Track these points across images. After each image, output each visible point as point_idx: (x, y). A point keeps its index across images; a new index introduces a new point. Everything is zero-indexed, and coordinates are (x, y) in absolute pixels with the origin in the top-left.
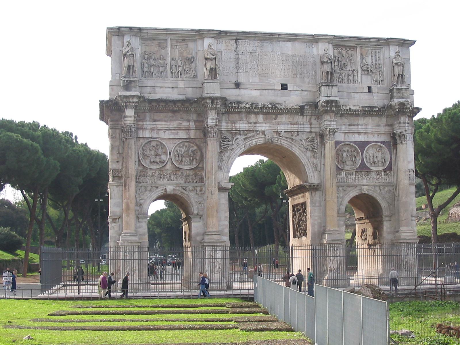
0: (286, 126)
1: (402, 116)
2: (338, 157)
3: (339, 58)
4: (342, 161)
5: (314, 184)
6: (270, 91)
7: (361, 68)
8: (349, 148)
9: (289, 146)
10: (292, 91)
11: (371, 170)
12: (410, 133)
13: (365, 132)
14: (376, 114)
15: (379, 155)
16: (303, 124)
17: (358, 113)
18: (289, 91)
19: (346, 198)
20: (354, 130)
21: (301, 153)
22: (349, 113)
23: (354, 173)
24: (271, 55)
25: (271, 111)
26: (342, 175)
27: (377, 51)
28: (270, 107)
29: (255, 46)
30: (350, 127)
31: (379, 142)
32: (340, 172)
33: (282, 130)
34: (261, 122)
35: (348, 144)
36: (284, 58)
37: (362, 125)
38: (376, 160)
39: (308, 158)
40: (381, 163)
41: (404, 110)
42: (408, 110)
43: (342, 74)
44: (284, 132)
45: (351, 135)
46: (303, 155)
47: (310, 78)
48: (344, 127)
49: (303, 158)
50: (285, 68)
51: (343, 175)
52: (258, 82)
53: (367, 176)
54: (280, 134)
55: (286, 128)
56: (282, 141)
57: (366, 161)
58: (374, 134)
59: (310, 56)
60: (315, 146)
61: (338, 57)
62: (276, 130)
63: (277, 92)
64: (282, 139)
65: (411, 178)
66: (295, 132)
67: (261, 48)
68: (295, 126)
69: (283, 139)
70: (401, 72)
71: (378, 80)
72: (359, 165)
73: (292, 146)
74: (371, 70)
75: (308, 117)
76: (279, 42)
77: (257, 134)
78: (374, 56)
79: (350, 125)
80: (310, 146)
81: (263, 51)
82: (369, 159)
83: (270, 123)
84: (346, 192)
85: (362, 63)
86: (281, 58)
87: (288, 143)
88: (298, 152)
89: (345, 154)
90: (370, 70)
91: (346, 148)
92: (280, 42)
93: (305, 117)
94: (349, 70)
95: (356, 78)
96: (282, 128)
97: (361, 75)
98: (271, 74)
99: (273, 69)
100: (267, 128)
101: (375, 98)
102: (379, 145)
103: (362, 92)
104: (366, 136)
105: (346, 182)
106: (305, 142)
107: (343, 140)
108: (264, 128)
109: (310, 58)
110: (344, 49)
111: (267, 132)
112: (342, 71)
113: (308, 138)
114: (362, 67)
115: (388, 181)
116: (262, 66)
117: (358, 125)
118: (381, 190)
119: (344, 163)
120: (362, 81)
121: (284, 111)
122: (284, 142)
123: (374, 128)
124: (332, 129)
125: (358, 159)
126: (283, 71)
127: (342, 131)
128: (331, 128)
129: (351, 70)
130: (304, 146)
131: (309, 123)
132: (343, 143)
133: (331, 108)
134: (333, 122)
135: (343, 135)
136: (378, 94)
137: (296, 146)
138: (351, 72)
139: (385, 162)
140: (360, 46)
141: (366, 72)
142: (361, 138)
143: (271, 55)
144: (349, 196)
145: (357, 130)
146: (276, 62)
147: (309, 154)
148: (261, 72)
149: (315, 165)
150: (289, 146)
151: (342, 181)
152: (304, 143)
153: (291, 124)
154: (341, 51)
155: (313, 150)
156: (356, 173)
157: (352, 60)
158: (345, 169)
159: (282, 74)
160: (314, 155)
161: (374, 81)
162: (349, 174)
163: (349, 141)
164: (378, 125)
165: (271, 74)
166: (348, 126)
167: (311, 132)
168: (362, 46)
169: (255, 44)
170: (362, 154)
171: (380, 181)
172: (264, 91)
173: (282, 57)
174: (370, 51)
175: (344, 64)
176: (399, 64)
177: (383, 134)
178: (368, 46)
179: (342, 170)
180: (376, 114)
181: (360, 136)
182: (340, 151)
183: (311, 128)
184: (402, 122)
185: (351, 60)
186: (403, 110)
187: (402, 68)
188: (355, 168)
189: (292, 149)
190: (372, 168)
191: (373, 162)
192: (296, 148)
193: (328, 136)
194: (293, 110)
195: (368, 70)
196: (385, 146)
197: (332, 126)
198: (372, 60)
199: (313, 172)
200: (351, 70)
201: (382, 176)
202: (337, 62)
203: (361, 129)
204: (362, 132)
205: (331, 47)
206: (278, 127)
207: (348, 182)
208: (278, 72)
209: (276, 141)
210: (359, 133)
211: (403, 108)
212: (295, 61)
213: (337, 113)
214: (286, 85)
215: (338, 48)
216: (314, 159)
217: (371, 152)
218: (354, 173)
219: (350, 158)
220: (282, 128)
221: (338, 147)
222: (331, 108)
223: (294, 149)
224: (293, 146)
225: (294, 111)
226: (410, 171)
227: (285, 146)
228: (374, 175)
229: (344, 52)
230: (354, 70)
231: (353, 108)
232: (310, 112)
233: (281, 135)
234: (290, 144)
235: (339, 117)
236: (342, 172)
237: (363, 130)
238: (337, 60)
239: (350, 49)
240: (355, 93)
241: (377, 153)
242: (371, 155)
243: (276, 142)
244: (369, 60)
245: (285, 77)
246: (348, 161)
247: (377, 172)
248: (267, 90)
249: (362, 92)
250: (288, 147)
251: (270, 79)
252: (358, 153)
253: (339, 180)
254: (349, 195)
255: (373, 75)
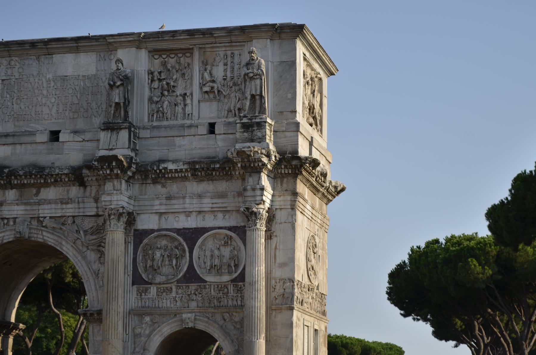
0: (53, 206)
1: (250, 176)
2: (146, 261)
3: (162, 74)
4: (152, 266)
5: (91, 312)
6: (29, 146)
7: (201, 88)
8: (168, 241)
9: (57, 243)
10: (68, 143)
11: (206, 282)
12: (289, 207)
13: (198, 210)
14: (218, 174)
15: (226, 252)
16: (84, 202)
17: (183, 175)
18: (61, 144)
19: (154, 336)
20: (176, 207)
21: (77, 255)
22: (166, 176)
23: (174, 289)
24: (36, 81)
25: (25, 182)
26: (150, 293)
27: (236, 53)
28: (22, 174)
29: (9, 66)
30: (168, 202)
31: (225, 228)
32: (146, 291)
33: (45, 215)
34: (9, 202)
35: (165, 235)
36: (59, 85)
37: (191, 198)
38: (217, 262)
39: (88, 263)
40: (226, 267)
41: (252, 165)
42: (260, 164)
43: (163, 103)
44: (51, 217)
45: (171, 217)
46: (80, 258)
47: (102, 115)
48: (157, 202)
49: (79, 265)
50: (59, 102)
51: (151, 294)
52: (12, 130)
53: (200, 294)
54: (42, 222)
55: (53, 211)
56: (44, 234)
57: (200, 267)
58: (216, 213)
59: (105, 76)
60: (102, 242)
61: (160, 73)
62: (36, 216)
63: (41, 147)
64: (44, 231)
65: (286, 296)
66: (69, 216)
67: (20, 70)
68: (70, 206)
69: (47, 232)
70: (256, 90)
71: (232, 108)
72: (181, 275)
73: (61, 243)
74: (219, 91)
75: (94, 188)
76: (50, 56)
77: (4, 223)
78: (229, 63)
79: (169, 198)
80: (93, 242)
81: (23, 75)
82: (205, 263)
83: (26, 204)
84: (156, 325)
85: (202, 78)
86: (52, 84)
87: (56, 238)
88: (71, 254)
89: (158, 254)
90: (216, 92)
91: (164, 242)
92: (54, 56)
93: (88, 189)
94: (177, 96)
95: (188, 109)
96: (46, 211)
97: (199, 102)
98: (34, 115)
99: (38, 106)
100: (21, 212)
101: (220, 143)
102: (227, 235)
103: (194, 135)
104: (200, 217)
105: (157, 305)
106: (85, 235)
107: (156, 227)
108: (15, 212)
109: (104, 79)
110: (173, 56)
111: (20, 219)
112: (163, 98)
113: (92, 228)
114: (202, 85)
115: (239, 303)
116: (19, 102)
117: (184, 198)
118: (225, 320)
119: (156, 270)
120: (201, 113)
121: (49, 181)
122: (49, 235)
123: (215, 201)
124: (112, 209)
125: (183, 261)
126: (55, 109)
127: (154, 211)
128: (112, 207)
129: (180, 95)
130: (82, 242)
131: (92, 200)
132: (156, 233)
133: (112, 170)
134: (115, 197)
135: (156, 217)
136: (226, 136)
137: (67, 242)
138: (181, 98)
139: (236, 266)
140: (200, 48)
141: (211, 96)
142: (192, 223)
143: (36, 81)
144: (160, 333)
145: (182, 206)
146: (45, 92)
147: (92, 256)
148: (18, 114)
149: (100, 275)
150: (57, 243)
151: (151, 305)
152: (83, 237)
153: (62, 203)
154: (166, 60)
155: (99, 248)
156: (178, 287)
157: (186, 75)
158: (153, 281)
159: (54, 114)
160: (100, 257)
161: (226, 112)
162: (164, 292)
163: (167, 230)
164: (222, 195)
165: (34, 115)
166: (164, 201)
167: (97, 215)
168: (203, 46)
169: (9, 64)
170: (191, 253)
171: (224, 302)
172: (18, 147)
173: (55, 84)
174: (222, 54)
175: (168, 84)
176: (251, 75)
177: (234, 213)
178: (215, 45)
179: (151, 284)
180: (218, 174)
181: (189, 218)
182: (151, 247)
183: (97, 208)
184: (249, 187)
185: (184, 74)
186: (250, 165)
187: (258, 81)
188: (176, 279)
189: (60, 248)
190: (209, 278)
191: (211, 267)
192: (69, 247)
193: (108, 222)
194: (63, 177)
195: (214, 92)
196: (238, 235)
197: (115, 203)
198: (225, 70)
199: (96, 290)
200: (180, 95)
201: (228, 293)
202: (157, 82)
203: (190, 204)
204: (191, 210)
205: (143, 54)
206: (39, 210)
207: (160, 306)
208: (46, 110)
209: (35, 236)
210: (188, 214)
211: (249, 161)
212: (77, 88)
213: (143, 177)
214: (58, 132)
215: (160, 56)
216: (100, 265)
217: (210, 245)
218: (174, 289)
219: (169, 261)
220: (46, 211)
221: (146, 241)
222: (112, 170)
223: (64, 248)
224: (64, 243)
225: (67, 180)
226: (284, 283)
227: (50, 244)
228: (212, 291)
229: (172, 61)
230: (185, 94)
231: (171, 166)
232: (94, 178)
233: (44, 225)
234: (60, 240)
235: (152, 185)
236: (150, 288)
237: (195, 205)
238: (156, 78)
239: (184, 54)
240: (181, 138)
241: (222, 248)
242: (208, 253)
243: (34, 237)
244: (219, 72)
245: (58, 119)
246: (165, 265)
247: (218, 286)
248: (23, 145)
249: (194, 135)
250: (55, 244)
251: (32, 125)
252: (184, 251)
253: (143, 303)
254: (160, 331)
255: (226, 100)
